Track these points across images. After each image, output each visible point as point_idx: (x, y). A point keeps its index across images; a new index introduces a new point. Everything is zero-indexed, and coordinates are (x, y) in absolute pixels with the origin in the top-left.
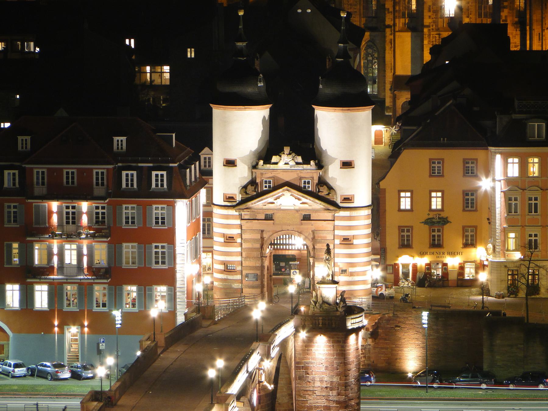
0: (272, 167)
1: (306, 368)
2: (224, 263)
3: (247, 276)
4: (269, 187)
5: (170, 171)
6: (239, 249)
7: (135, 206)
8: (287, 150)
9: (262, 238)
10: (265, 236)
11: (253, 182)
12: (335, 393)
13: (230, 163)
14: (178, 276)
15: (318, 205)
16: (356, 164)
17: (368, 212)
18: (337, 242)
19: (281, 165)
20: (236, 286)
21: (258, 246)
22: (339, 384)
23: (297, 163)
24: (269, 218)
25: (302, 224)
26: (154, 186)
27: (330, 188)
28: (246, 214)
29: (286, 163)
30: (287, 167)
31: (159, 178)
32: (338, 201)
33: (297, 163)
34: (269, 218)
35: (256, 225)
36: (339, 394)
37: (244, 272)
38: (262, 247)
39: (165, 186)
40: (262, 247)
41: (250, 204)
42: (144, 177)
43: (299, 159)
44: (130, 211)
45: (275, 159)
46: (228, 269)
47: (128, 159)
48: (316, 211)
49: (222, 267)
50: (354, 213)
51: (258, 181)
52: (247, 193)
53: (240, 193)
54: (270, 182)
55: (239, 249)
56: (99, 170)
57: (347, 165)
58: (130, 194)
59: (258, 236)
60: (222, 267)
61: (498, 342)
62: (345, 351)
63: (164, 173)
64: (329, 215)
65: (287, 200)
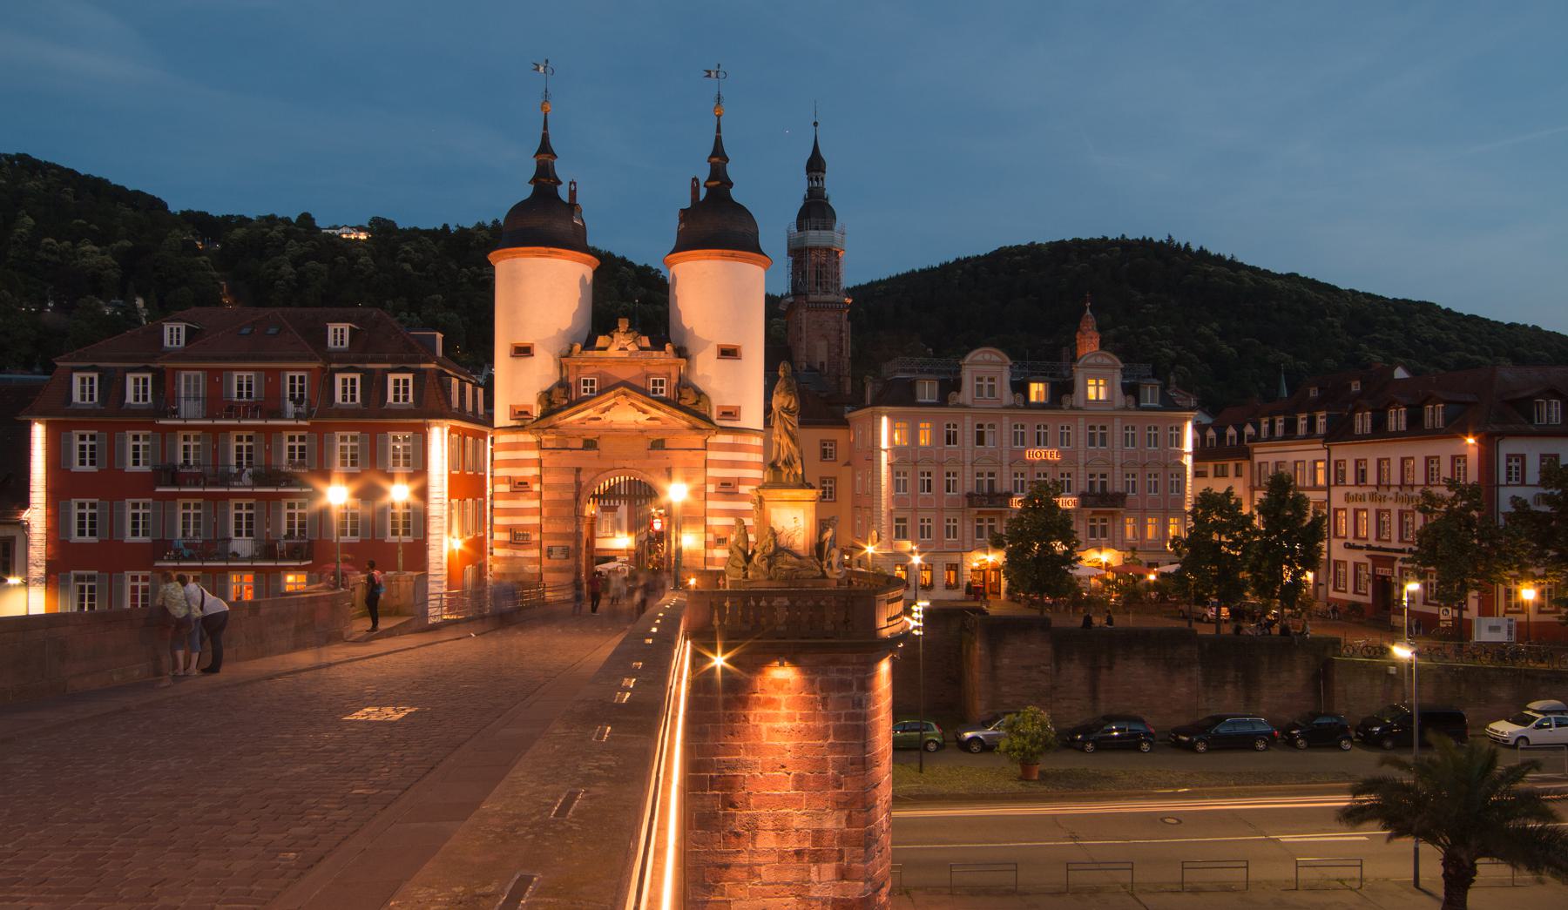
0: (597, 354)
1: (729, 784)
2: (510, 529)
3: (550, 551)
4: (592, 390)
5: (420, 375)
6: (536, 504)
7: (357, 433)
8: (623, 324)
9: (578, 484)
10: (584, 478)
11: (563, 384)
12: (829, 869)
13: (523, 351)
14: (432, 555)
15: (680, 421)
16: (744, 352)
17: (757, 441)
18: (711, 488)
19: (613, 351)
20: (532, 568)
21: (570, 496)
22: (844, 839)
23: (642, 349)
24: (590, 444)
25: (649, 456)
26: (390, 399)
27: (700, 394)
28: (549, 439)
29: (620, 346)
30: (625, 354)
31: (398, 385)
32: (714, 416)
33: (642, 349)
34: (590, 444)
35: (567, 459)
36: (843, 874)
37: (545, 545)
38: (577, 499)
39: (411, 400)
40: (577, 499)
41: (555, 419)
42: (375, 385)
43: (646, 342)
44: (349, 444)
45: (601, 341)
46: (517, 538)
47: (347, 360)
48: (675, 432)
49: (505, 537)
50: (740, 440)
51: (572, 380)
52: (550, 402)
53: (540, 401)
54: (592, 383)
55: (536, 504)
56: (295, 374)
57: (728, 353)
58: (348, 417)
59: (571, 479)
60: (505, 537)
61: (1006, 661)
62: (865, 717)
63: (410, 377)
64: (696, 440)
65: (625, 415)
